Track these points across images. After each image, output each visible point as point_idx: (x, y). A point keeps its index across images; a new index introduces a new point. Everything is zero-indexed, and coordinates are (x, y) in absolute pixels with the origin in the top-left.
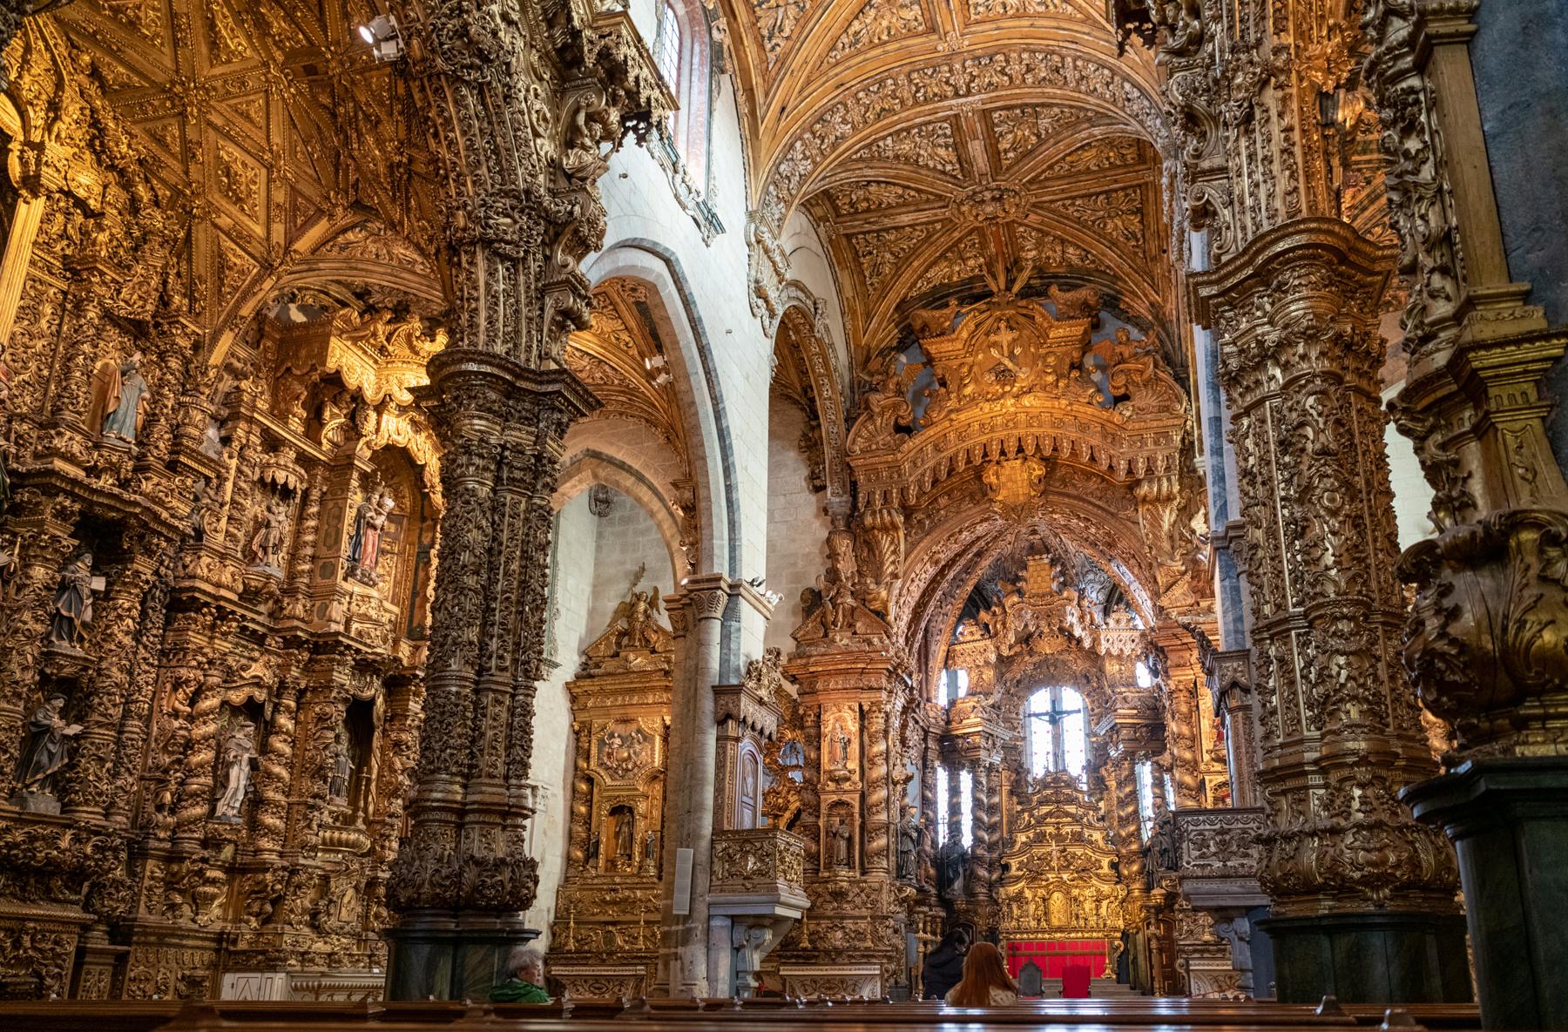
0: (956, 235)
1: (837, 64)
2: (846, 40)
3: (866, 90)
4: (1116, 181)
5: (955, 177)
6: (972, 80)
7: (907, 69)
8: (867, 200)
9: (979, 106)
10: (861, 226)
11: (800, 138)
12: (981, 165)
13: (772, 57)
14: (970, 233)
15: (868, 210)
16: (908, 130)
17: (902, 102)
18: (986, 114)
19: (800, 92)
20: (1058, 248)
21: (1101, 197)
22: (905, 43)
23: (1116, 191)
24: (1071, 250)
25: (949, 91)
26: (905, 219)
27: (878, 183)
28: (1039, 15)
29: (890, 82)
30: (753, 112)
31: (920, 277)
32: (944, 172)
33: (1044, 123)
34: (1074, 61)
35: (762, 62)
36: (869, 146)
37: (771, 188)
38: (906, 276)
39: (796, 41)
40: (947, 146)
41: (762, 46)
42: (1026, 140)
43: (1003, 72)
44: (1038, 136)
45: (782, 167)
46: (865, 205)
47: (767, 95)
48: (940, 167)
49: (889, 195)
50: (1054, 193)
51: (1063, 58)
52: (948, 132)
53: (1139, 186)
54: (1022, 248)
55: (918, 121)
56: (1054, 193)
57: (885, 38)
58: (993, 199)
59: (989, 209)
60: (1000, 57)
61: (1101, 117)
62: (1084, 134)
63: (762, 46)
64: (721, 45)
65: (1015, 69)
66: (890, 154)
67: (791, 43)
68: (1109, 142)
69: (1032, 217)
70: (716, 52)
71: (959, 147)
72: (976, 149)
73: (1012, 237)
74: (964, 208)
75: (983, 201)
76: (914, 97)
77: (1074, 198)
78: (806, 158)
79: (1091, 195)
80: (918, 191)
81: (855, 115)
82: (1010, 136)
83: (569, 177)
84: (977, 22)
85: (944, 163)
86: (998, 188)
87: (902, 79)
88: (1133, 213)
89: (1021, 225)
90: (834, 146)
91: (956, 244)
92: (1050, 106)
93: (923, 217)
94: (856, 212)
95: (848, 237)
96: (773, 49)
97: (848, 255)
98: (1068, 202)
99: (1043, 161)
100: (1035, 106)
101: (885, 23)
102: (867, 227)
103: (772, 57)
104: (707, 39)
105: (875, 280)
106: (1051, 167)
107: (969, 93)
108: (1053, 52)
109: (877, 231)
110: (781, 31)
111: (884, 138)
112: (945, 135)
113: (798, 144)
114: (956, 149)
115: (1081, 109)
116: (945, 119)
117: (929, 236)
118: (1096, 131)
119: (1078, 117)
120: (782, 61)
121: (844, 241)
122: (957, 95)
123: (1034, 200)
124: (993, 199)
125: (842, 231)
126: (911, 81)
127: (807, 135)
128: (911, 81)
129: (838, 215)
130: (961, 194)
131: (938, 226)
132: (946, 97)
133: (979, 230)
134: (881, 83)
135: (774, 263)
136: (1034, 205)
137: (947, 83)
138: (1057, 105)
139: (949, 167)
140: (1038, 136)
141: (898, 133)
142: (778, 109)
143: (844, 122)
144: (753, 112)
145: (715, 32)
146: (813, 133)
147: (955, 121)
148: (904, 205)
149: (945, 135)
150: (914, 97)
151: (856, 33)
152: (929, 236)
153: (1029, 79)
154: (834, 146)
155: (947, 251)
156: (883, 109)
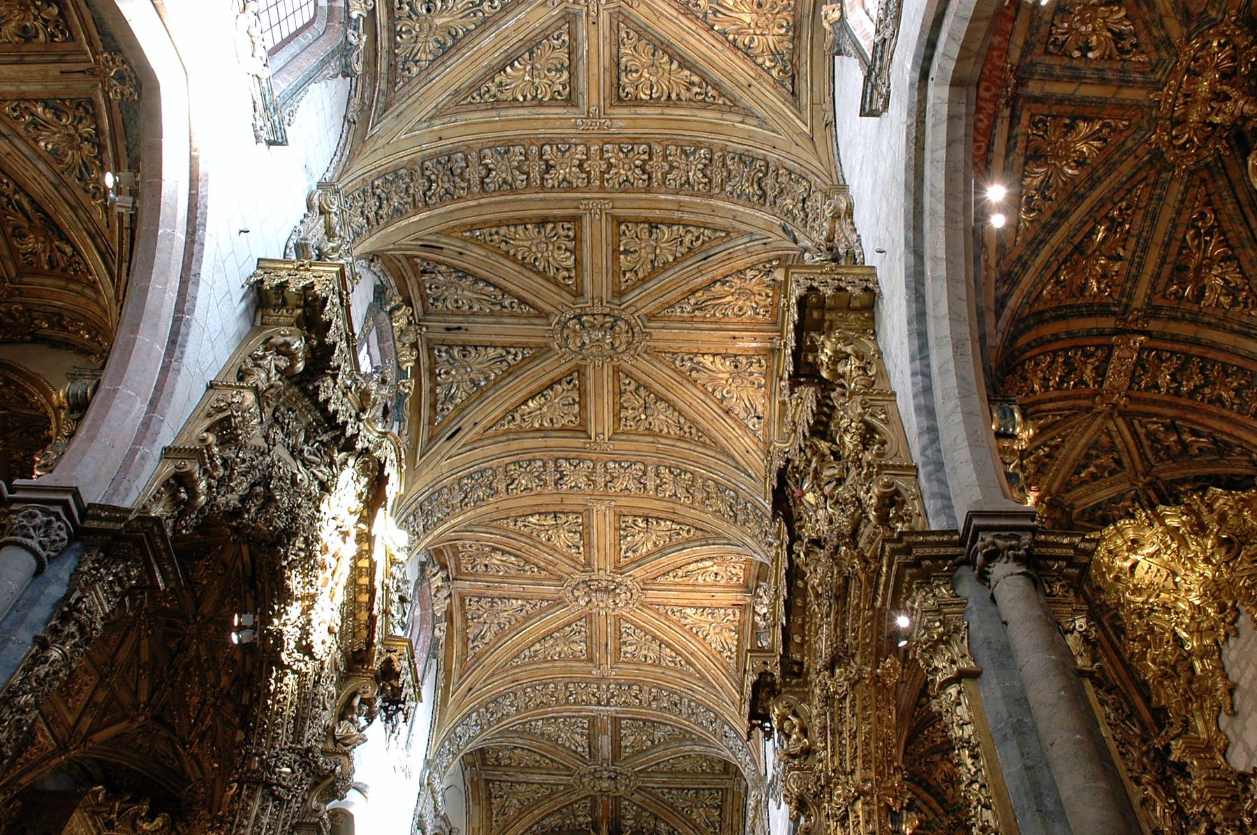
0: (574, 798)
1: (517, 666)
2: (528, 654)
3: (534, 688)
4: (705, 783)
5: (583, 757)
6: (613, 696)
7: (567, 680)
8: (510, 758)
9: (614, 714)
10: (500, 776)
11: (477, 711)
12: (605, 749)
13: (471, 653)
14: (585, 798)
15: (509, 766)
16: (556, 719)
17: (557, 700)
18: (616, 721)
19: (485, 681)
20: (652, 822)
21: (691, 792)
22: (569, 664)
23: (703, 789)
24: (662, 825)
25: (594, 700)
26: (537, 778)
27: (523, 749)
28: (668, 667)
29: (552, 685)
30: (447, 687)
31: (536, 823)
32: (575, 752)
33: (658, 734)
34: (690, 701)
35: (463, 654)
36: (524, 724)
37: (447, 743)
38: (525, 820)
39: (491, 647)
40: (582, 735)
41: (465, 645)
42: (643, 742)
43: (636, 697)
44: (653, 742)
45: (459, 729)
46: (508, 761)
47: (460, 677)
48: (573, 748)
49: (527, 759)
50: (657, 782)
51: (681, 698)
52: (586, 726)
53: (722, 789)
54: (623, 817)
55: (565, 714)
56: (657, 782)
57: (556, 658)
58: (609, 778)
59: (605, 785)
60: (635, 687)
61: (701, 740)
62: (686, 748)
63: (465, 645)
64: (438, 640)
65: (645, 696)
66: (538, 732)
67: (487, 647)
68: (706, 758)
69: (636, 796)
70: (435, 642)
71: (591, 738)
72: (605, 742)
73: (617, 808)
74: (584, 780)
75: (601, 778)
76: (567, 698)
77: (671, 789)
78: (477, 725)
79: (683, 789)
80: (552, 760)
81: (521, 702)
82: (632, 738)
83: (336, 741)
84: (624, 662)
85: (577, 745)
86: (615, 771)
87: (561, 686)
88: (714, 808)
89: (626, 799)
90: (499, 720)
91: (571, 804)
92: (666, 725)
93: (551, 779)
94: (499, 765)
95: (487, 782)
96: (474, 648)
97: (483, 795)
98: (666, 791)
99: (653, 759)
100: (653, 722)
101: (558, 649)
102: (504, 778)
103: (471, 653)
104: (430, 635)
105: (500, 818)
106: (657, 764)
107: (608, 704)
108: (675, 693)
109: (511, 782)
110: (483, 637)
111: (537, 720)
112: (583, 728)
113: (474, 714)
114: (588, 738)
115: (688, 731)
116: (585, 717)
117: (552, 793)
118: (697, 748)
119: (684, 736)
120: (477, 657)
121: (482, 784)
122: (599, 704)
123: (640, 784)
124: (609, 778)
125: (483, 776)
126: (567, 688)
127: (482, 710)
128: (567, 688)
129: (484, 764)
130: (585, 769)
131: (561, 788)
132: (590, 704)
133: (594, 799)
134: (546, 685)
135: (436, 802)
136: (639, 788)
137: (594, 695)
138: (671, 725)
139: (580, 749)
140: (653, 742)
141: (548, 719)
142: (467, 689)
143: (512, 705)
144: (447, 687)
145: (437, 630)
146: (487, 710)
147: (592, 720)
148: (538, 768)
149: (583, 728)
150: (567, 698)
151: (536, 651)
152: (552, 793)
153: (654, 705)
154: (499, 720)
155: (563, 807)
156: (542, 702)
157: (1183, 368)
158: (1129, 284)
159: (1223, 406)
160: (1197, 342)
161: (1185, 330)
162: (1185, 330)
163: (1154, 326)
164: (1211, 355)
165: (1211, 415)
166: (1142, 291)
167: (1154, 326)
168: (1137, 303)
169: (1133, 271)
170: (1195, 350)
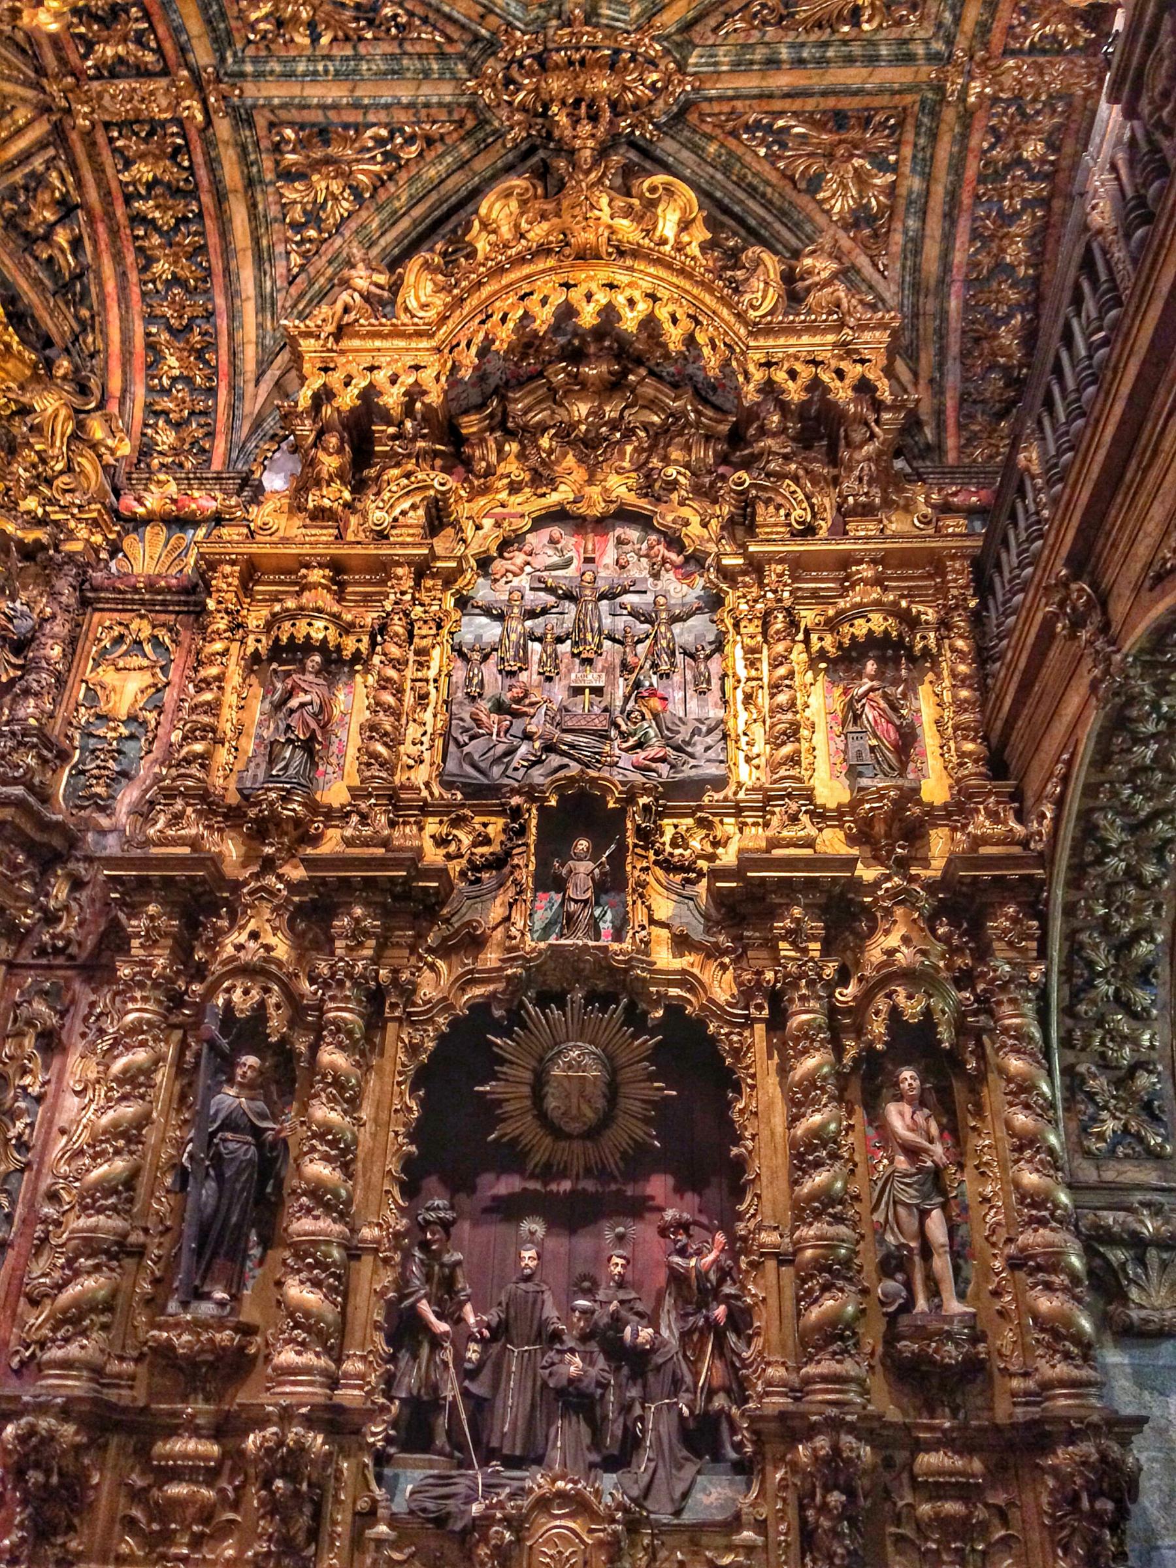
157: (175, 191)
158: (278, 68)
159: (145, 269)
160: (220, 197)
161: (232, 174)
162: (232, 174)
163: (223, 127)
164: (209, 224)
165: (118, 258)
166: (277, 92)
167: (223, 127)
168: (250, 89)
169: (301, 67)
170: (207, 199)
